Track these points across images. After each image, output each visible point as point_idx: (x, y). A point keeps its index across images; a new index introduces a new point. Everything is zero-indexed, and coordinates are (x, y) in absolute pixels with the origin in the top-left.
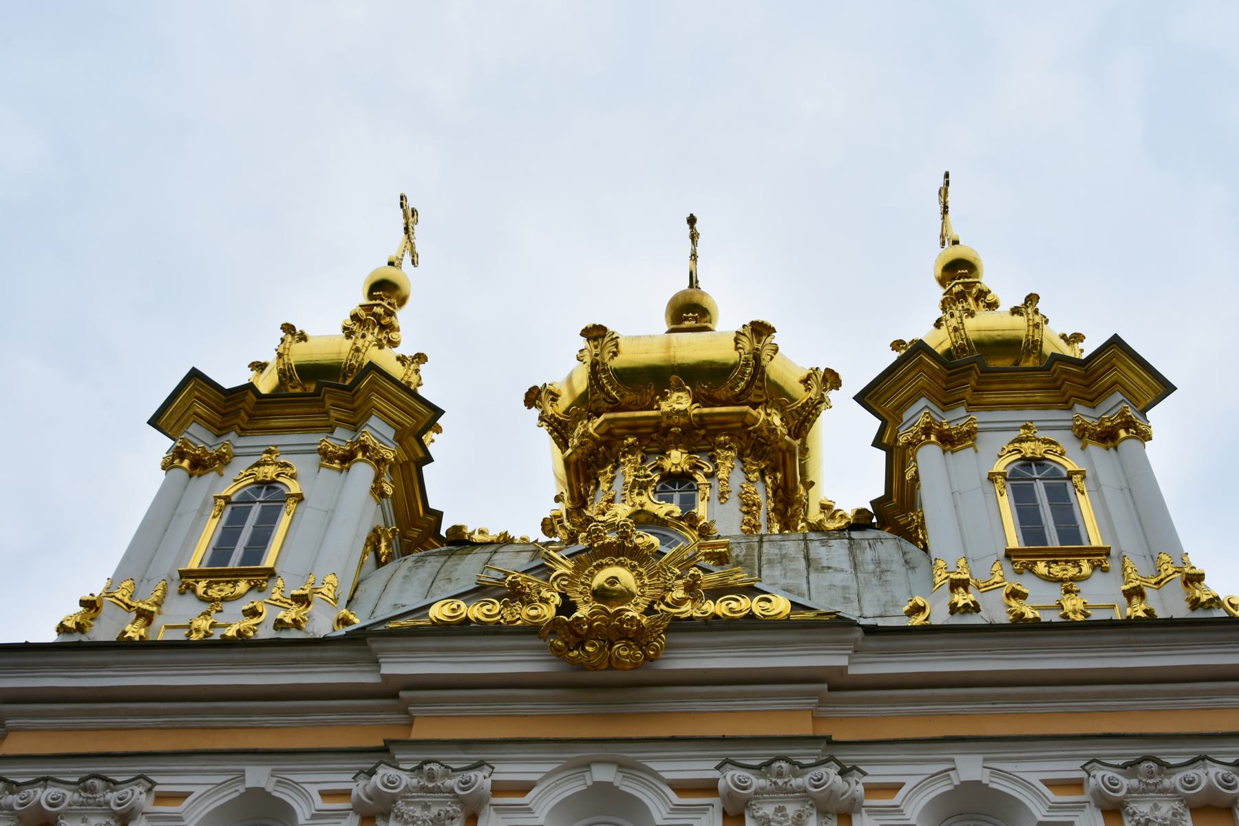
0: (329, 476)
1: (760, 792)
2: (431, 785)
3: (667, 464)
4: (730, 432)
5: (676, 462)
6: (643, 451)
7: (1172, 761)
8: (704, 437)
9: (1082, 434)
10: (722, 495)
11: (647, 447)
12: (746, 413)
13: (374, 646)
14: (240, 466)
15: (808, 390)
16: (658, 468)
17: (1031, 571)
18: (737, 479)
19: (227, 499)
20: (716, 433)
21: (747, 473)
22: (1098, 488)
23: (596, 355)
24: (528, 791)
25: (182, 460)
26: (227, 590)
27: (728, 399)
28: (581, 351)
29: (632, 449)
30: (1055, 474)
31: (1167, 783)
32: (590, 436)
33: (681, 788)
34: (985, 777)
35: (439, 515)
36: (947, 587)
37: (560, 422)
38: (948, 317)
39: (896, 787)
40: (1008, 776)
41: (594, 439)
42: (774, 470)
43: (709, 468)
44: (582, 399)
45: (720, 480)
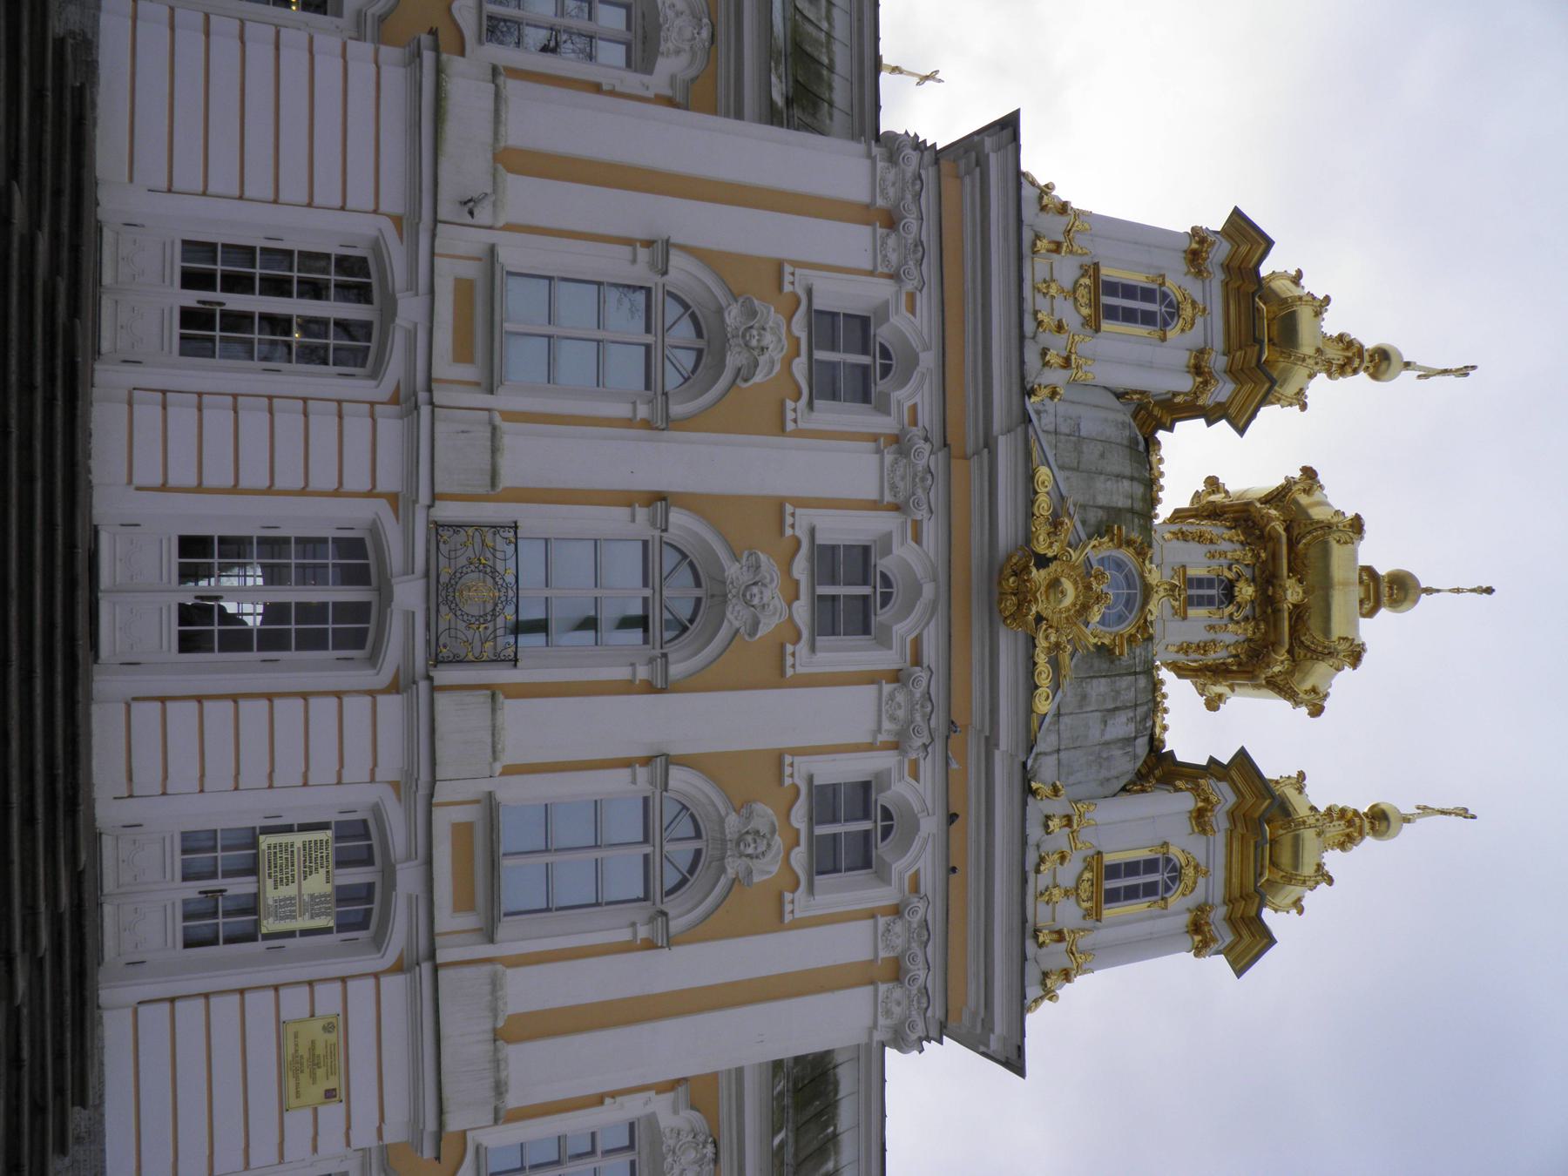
0: (1184, 358)
1: (911, 694)
2: (917, 480)
5: (1243, 591)
6: (1254, 565)
8: (1265, 612)
10: (1212, 627)
13: (1019, 429)
14: (1194, 289)
15: (1306, 692)
16: (1239, 576)
17: (1086, 868)
18: (1228, 638)
20: (1267, 623)
22: (1152, 918)
23: (1337, 527)
24: (917, 542)
26: (1083, 301)
28: (1343, 513)
29: (1258, 556)
30: (1168, 889)
32: (1268, 523)
33: (917, 643)
35: (1170, 429)
36: (1070, 812)
37: (1284, 496)
38: (1317, 817)
39: (916, 777)
41: (1266, 526)
42: (1240, 664)
43: (1237, 617)
44: (1303, 511)
45: (1226, 625)
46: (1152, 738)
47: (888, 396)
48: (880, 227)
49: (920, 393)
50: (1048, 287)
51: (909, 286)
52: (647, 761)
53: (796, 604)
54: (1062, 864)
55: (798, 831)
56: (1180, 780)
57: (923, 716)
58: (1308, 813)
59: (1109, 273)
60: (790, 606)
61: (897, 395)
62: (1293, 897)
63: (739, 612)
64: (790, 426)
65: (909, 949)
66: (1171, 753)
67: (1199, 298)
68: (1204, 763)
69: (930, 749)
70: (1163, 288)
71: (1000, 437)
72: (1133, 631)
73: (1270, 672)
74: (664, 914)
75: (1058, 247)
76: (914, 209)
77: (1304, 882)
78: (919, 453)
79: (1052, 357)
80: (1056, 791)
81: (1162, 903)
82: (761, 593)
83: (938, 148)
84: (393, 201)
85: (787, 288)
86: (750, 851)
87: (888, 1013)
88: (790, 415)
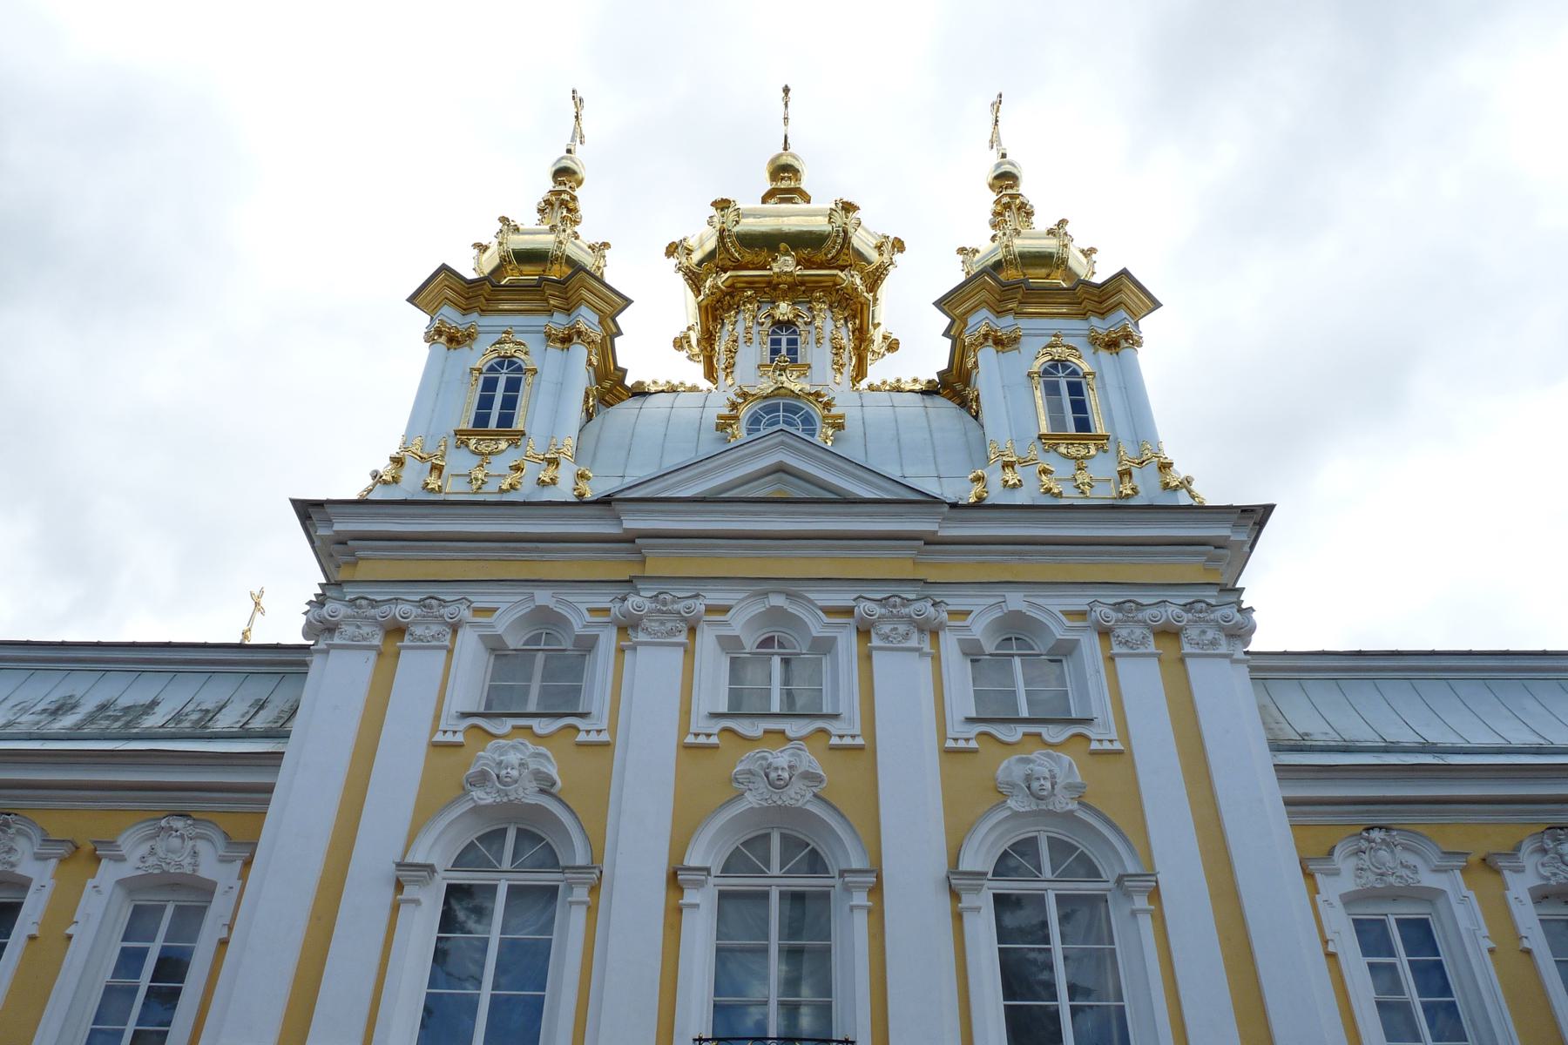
0: (554, 353)
2: (664, 609)
4: (825, 290)
6: (758, 301)
7: (1145, 601)
8: (804, 292)
9: (1095, 341)
11: (761, 298)
12: (836, 275)
15: (881, 255)
17: (1055, 450)
19: (480, 371)
20: (813, 290)
21: (836, 321)
22: (1104, 387)
23: (723, 223)
24: (728, 611)
26: (493, 446)
27: (822, 263)
28: (711, 217)
29: (750, 300)
30: (1074, 373)
31: (1140, 616)
32: (718, 288)
34: (1024, 608)
35: (624, 372)
36: (999, 464)
37: (694, 273)
38: (1001, 234)
41: (721, 290)
42: (855, 317)
44: (711, 256)
45: (816, 328)
46: (923, 392)
48: (402, 641)
50: (477, 479)
51: (466, 614)
52: (955, 895)
53: (790, 733)
54: (1051, 472)
55: (1025, 735)
57: (904, 606)
60: (790, 740)
61: (578, 629)
62: (1081, 256)
63: (796, 793)
64: (604, 737)
65: (1145, 622)
66: (940, 374)
67: (497, 337)
68: (948, 342)
69: (938, 600)
70: (484, 371)
71: (624, 526)
73: (861, 288)
74: (1120, 879)
75: (434, 467)
76: (385, 608)
77: (1065, 246)
78: (639, 608)
80: (979, 479)
82: (777, 769)
83: (325, 582)
85: (459, 738)
86: (1048, 785)
87: (1214, 643)
88: (593, 737)
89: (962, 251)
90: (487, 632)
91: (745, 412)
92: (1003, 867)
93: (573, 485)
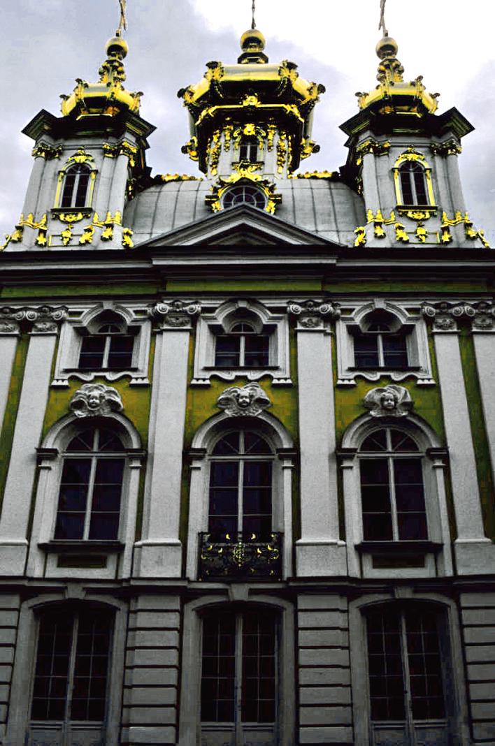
0: (108, 162)
3: (246, 132)
7: (452, 303)
9: (431, 151)
19: (64, 172)
25: (41, 153)
26: (74, 218)
29: (229, 123)
31: (450, 311)
33: (273, 310)
36: (373, 224)
38: (382, 85)
39: (351, 310)
40: (394, 307)
43: (264, 134)
44: (204, 97)
47: (130, 328)
49: (129, 309)
53: (250, 378)
55: (382, 377)
56: (356, 162)
58: (380, 89)
59: (57, 204)
62: (430, 98)
64: (146, 381)
66: (341, 169)
68: (347, 149)
72: (267, 189)
75: (43, 232)
76: (20, 313)
77: (421, 92)
78: (163, 310)
79: (106, 235)
81: (428, 172)
82: (242, 397)
84: (14, 601)
85: (66, 383)
88: (140, 382)
89: (358, 94)
90: (77, 325)
91: (221, 193)
92: (367, 446)
93: (121, 240)
